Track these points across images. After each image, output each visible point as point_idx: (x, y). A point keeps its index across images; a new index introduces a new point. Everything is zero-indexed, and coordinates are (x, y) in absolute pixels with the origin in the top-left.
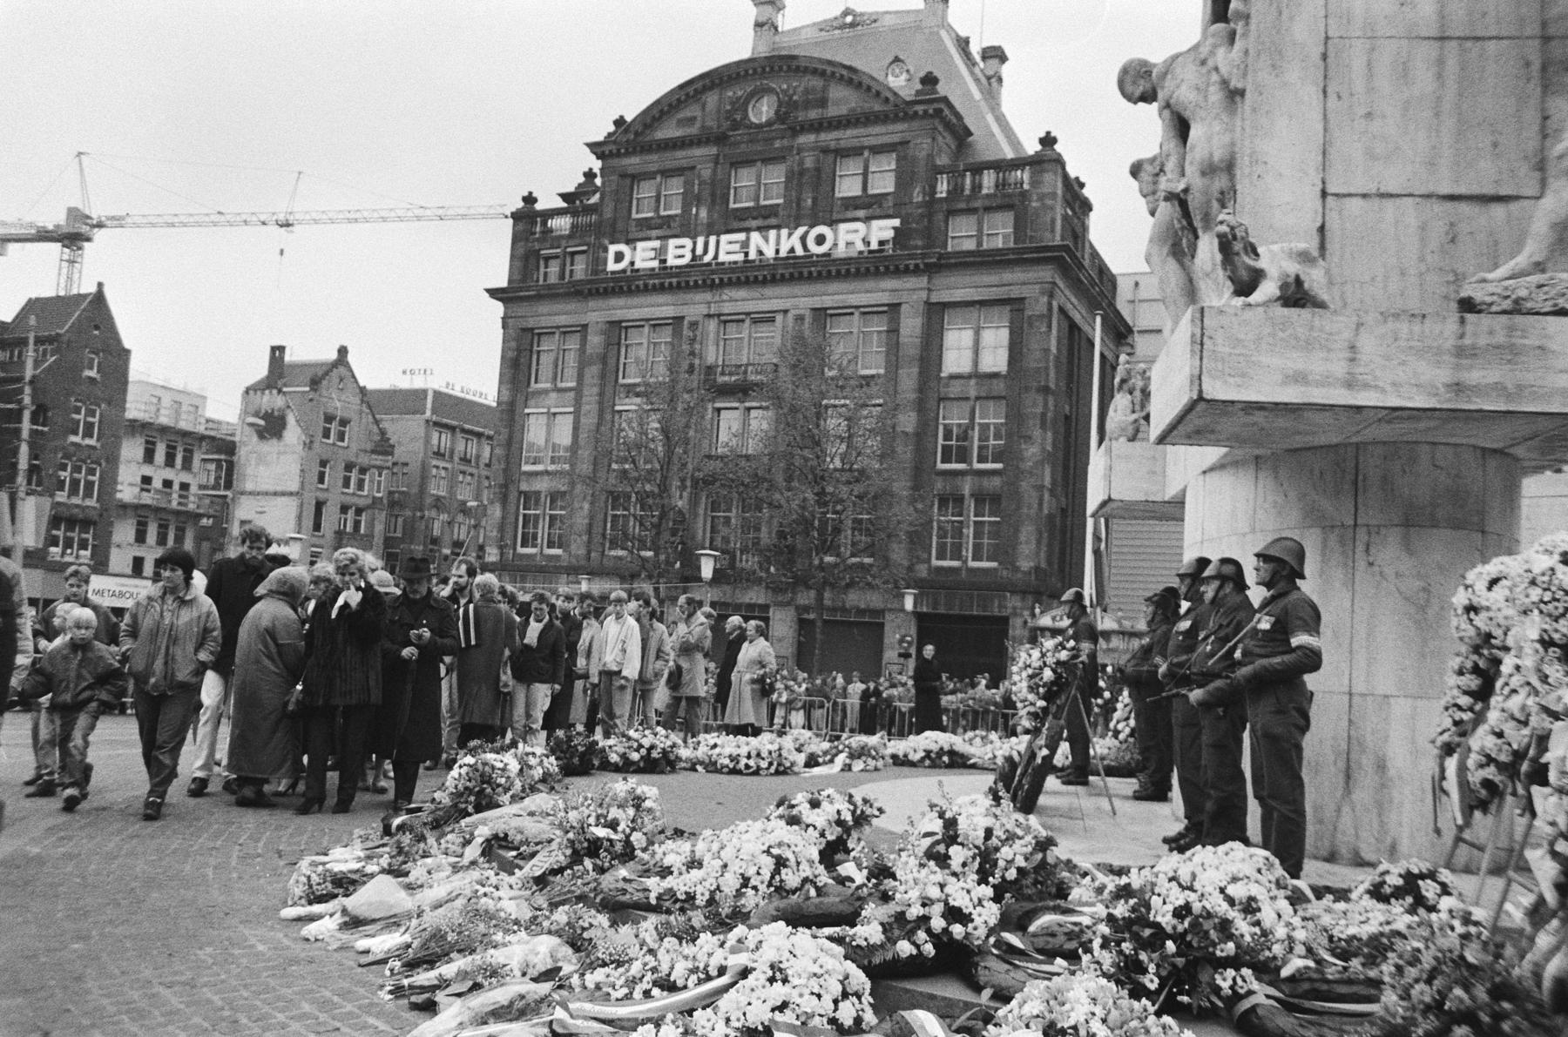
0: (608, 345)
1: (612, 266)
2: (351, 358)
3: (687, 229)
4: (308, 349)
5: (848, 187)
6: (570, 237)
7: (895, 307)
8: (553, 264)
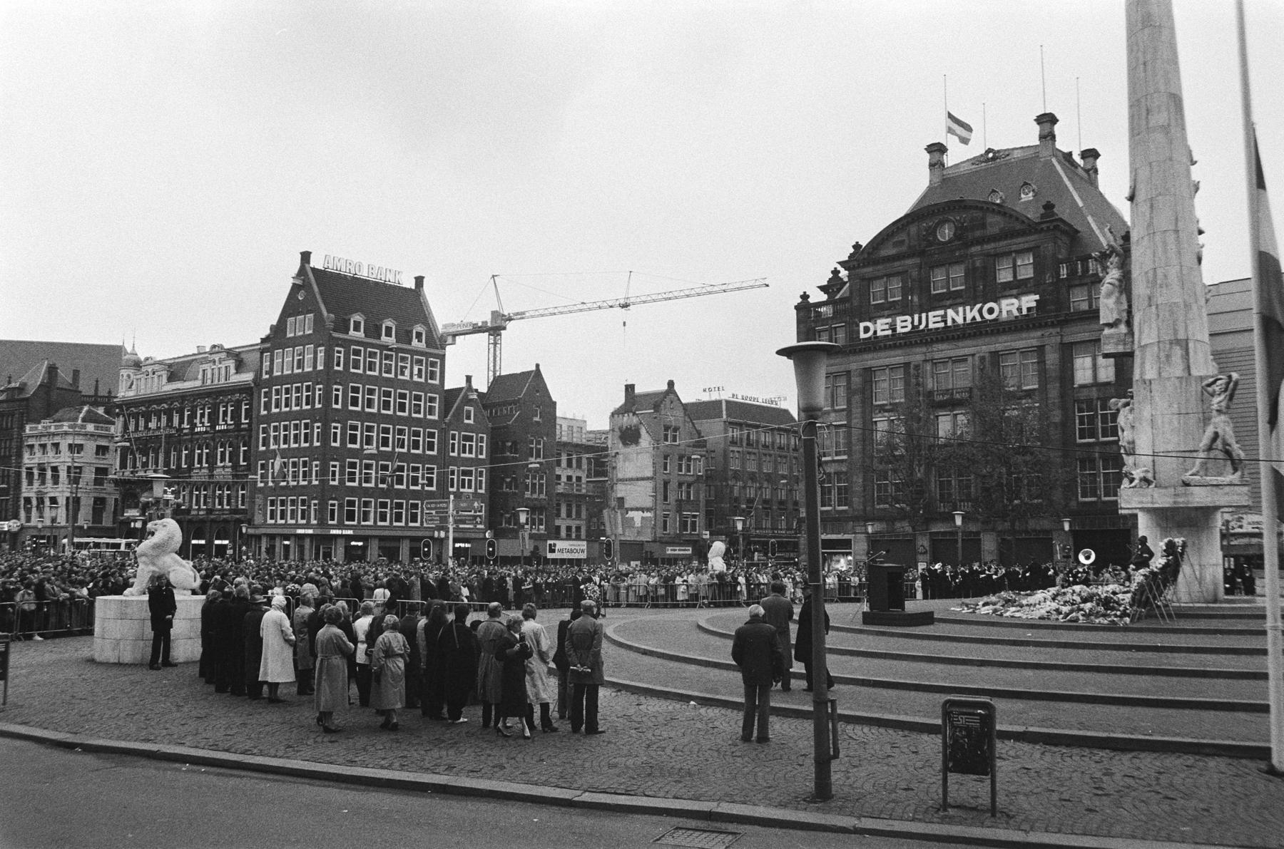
0: (865, 382)
1: (862, 336)
2: (676, 388)
3: (906, 309)
4: (649, 385)
5: (1005, 276)
6: (832, 318)
7: (1040, 350)
8: (824, 333)
